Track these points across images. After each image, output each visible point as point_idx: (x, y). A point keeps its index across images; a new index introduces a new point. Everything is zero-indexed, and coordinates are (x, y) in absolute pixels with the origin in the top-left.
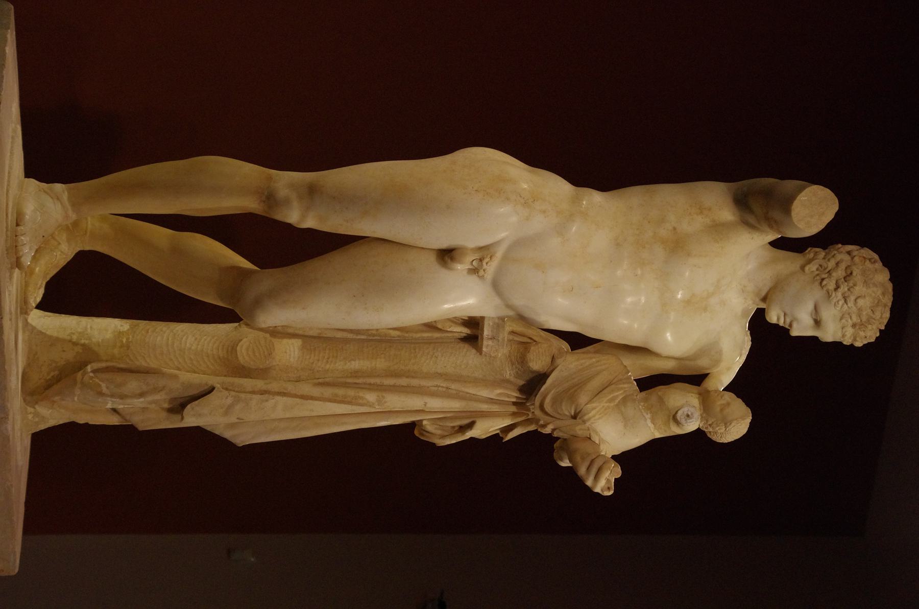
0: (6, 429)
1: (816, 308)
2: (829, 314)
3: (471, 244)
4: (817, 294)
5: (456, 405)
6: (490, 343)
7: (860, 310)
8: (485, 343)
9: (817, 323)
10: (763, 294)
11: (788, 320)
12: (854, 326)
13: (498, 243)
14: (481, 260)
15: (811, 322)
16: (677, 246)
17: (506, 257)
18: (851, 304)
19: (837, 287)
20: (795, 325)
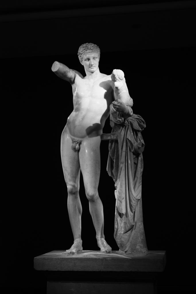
0: (109, 259)
1: (85, 60)
2: (85, 57)
3: (71, 144)
4: (83, 61)
5: (125, 144)
6: (112, 137)
7: (83, 50)
8: (113, 138)
9: (89, 59)
10: (91, 73)
11: (91, 66)
12: (86, 50)
13: (71, 138)
14: (75, 141)
15: (90, 61)
16: (78, 96)
17: (74, 136)
18: (82, 53)
19: (81, 57)
20: (91, 64)
